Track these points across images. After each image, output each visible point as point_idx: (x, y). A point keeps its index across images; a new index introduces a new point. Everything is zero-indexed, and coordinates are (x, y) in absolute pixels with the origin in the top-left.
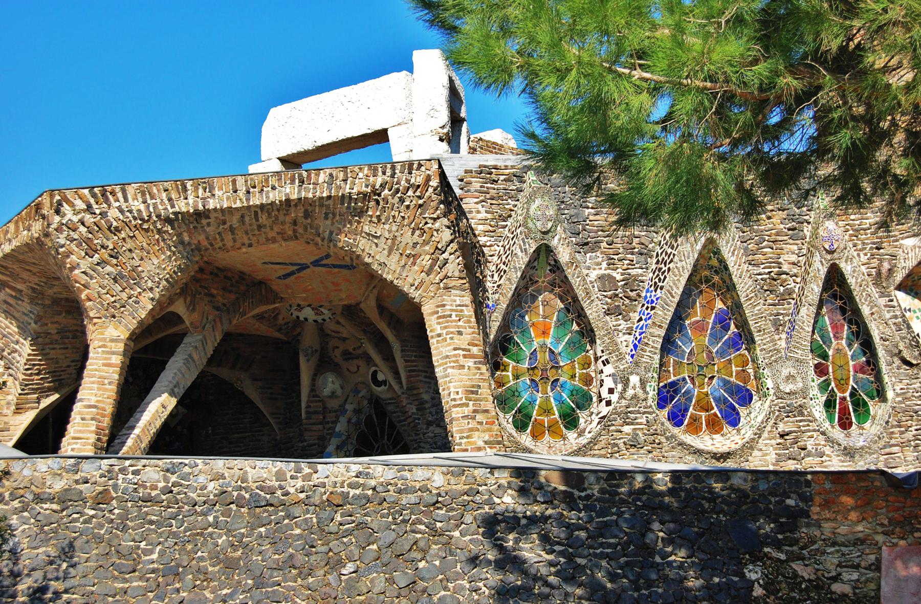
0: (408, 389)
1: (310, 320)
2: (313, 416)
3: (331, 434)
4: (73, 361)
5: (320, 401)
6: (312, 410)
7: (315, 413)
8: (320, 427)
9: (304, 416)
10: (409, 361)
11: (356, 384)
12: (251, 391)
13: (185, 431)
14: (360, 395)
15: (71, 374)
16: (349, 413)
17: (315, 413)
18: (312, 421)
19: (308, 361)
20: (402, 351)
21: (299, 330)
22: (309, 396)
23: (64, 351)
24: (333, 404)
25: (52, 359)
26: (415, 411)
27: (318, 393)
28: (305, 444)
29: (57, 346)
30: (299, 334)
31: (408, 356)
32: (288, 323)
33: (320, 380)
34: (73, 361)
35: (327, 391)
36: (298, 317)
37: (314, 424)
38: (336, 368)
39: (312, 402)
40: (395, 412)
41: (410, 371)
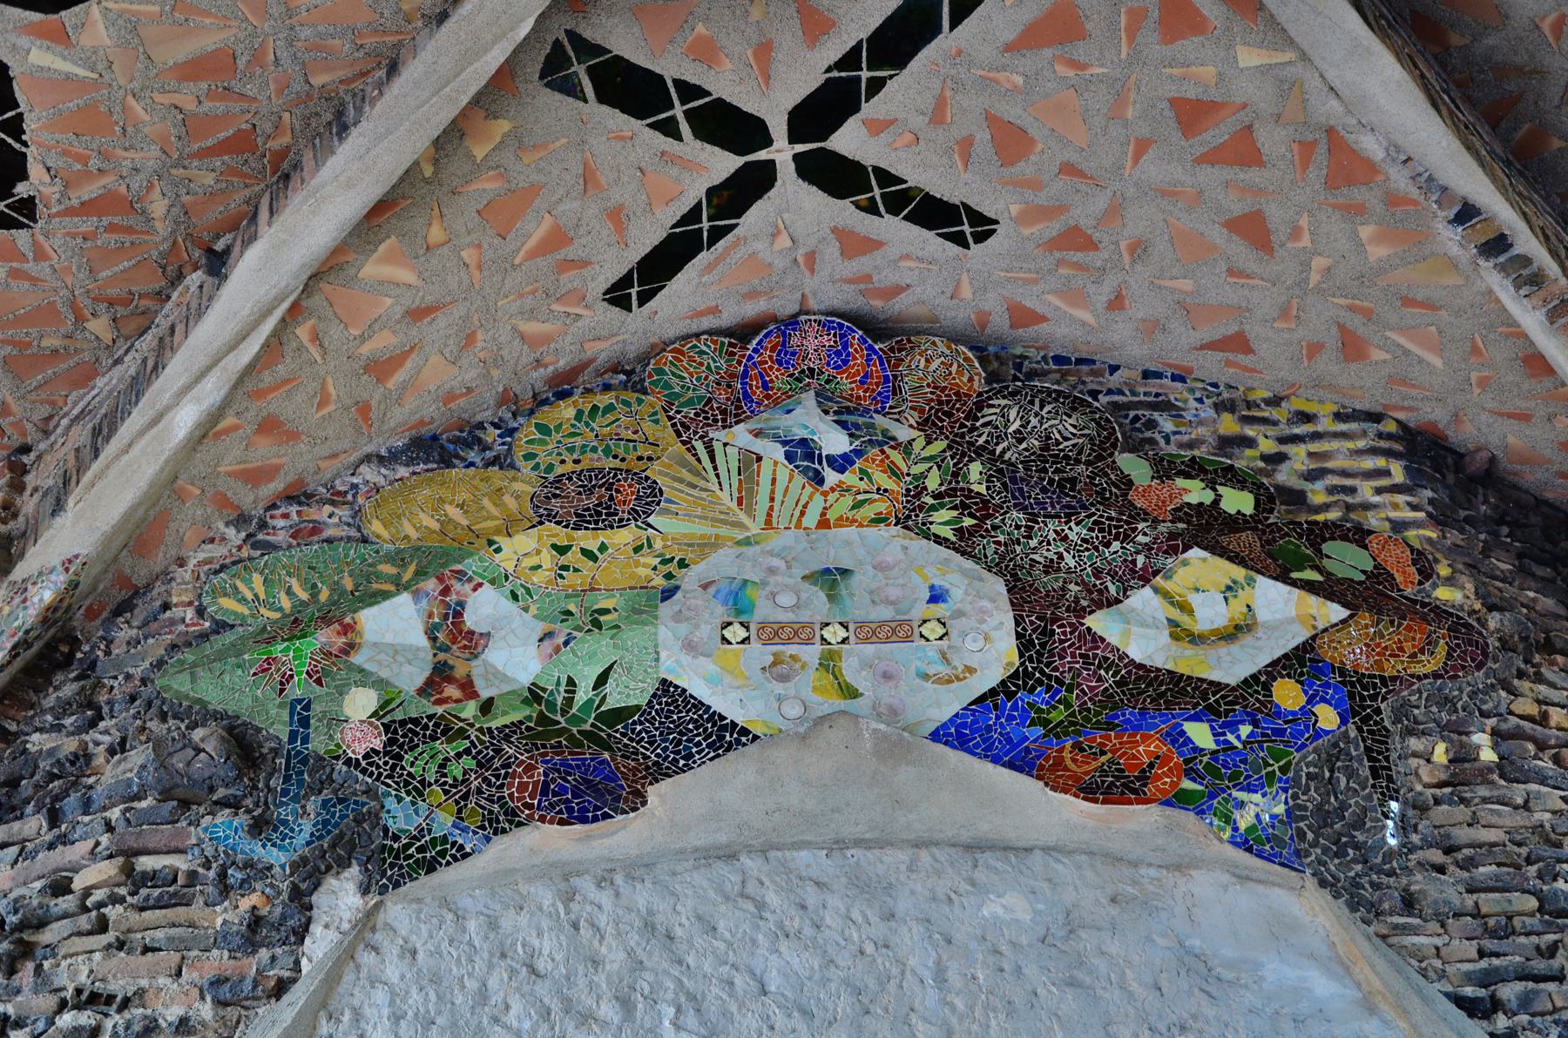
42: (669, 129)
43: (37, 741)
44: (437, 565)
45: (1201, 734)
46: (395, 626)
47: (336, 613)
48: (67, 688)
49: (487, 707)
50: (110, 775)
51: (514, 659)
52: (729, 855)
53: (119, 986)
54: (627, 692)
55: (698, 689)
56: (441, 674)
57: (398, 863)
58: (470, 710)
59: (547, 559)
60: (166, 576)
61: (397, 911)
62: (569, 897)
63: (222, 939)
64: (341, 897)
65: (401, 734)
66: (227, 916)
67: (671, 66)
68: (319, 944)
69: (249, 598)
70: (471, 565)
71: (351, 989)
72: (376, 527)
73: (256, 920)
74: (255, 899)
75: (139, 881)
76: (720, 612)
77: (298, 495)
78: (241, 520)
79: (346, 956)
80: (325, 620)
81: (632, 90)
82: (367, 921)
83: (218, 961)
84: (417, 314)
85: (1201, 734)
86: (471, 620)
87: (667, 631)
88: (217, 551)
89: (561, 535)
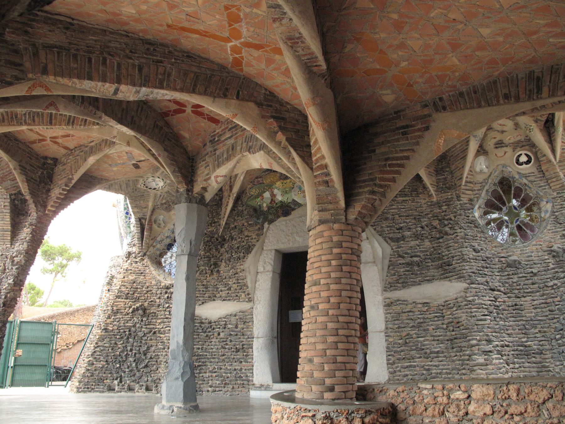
0: (560, 161)
2: (469, 184)
6: (468, 180)
9: (463, 183)
11: (498, 166)
18: (467, 188)
35: (478, 169)
37: (469, 190)
40: (535, 181)
43: (239, 208)
44: (270, 187)
46: (267, 195)
47: (260, 195)
48: (240, 203)
49: (276, 204)
50: (245, 213)
51: (279, 198)
52: (301, 217)
53: (249, 235)
54: (290, 200)
55: (296, 200)
56: (272, 200)
57: (271, 222)
58: (275, 205)
59: (281, 185)
60: (246, 189)
61: (271, 226)
62: (286, 223)
63: (257, 230)
64: (266, 225)
65: (269, 208)
66: (257, 228)
68: (265, 230)
69: (254, 192)
70: (274, 187)
71: (268, 234)
72: (264, 182)
73: (259, 228)
74: (258, 226)
75: (250, 225)
76: (298, 190)
77: (257, 178)
78: (251, 182)
79: (267, 231)
80: (261, 195)
82: (269, 227)
83: (257, 232)
86: (275, 193)
87: (293, 193)
88: (250, 186)
89: (282, 181)
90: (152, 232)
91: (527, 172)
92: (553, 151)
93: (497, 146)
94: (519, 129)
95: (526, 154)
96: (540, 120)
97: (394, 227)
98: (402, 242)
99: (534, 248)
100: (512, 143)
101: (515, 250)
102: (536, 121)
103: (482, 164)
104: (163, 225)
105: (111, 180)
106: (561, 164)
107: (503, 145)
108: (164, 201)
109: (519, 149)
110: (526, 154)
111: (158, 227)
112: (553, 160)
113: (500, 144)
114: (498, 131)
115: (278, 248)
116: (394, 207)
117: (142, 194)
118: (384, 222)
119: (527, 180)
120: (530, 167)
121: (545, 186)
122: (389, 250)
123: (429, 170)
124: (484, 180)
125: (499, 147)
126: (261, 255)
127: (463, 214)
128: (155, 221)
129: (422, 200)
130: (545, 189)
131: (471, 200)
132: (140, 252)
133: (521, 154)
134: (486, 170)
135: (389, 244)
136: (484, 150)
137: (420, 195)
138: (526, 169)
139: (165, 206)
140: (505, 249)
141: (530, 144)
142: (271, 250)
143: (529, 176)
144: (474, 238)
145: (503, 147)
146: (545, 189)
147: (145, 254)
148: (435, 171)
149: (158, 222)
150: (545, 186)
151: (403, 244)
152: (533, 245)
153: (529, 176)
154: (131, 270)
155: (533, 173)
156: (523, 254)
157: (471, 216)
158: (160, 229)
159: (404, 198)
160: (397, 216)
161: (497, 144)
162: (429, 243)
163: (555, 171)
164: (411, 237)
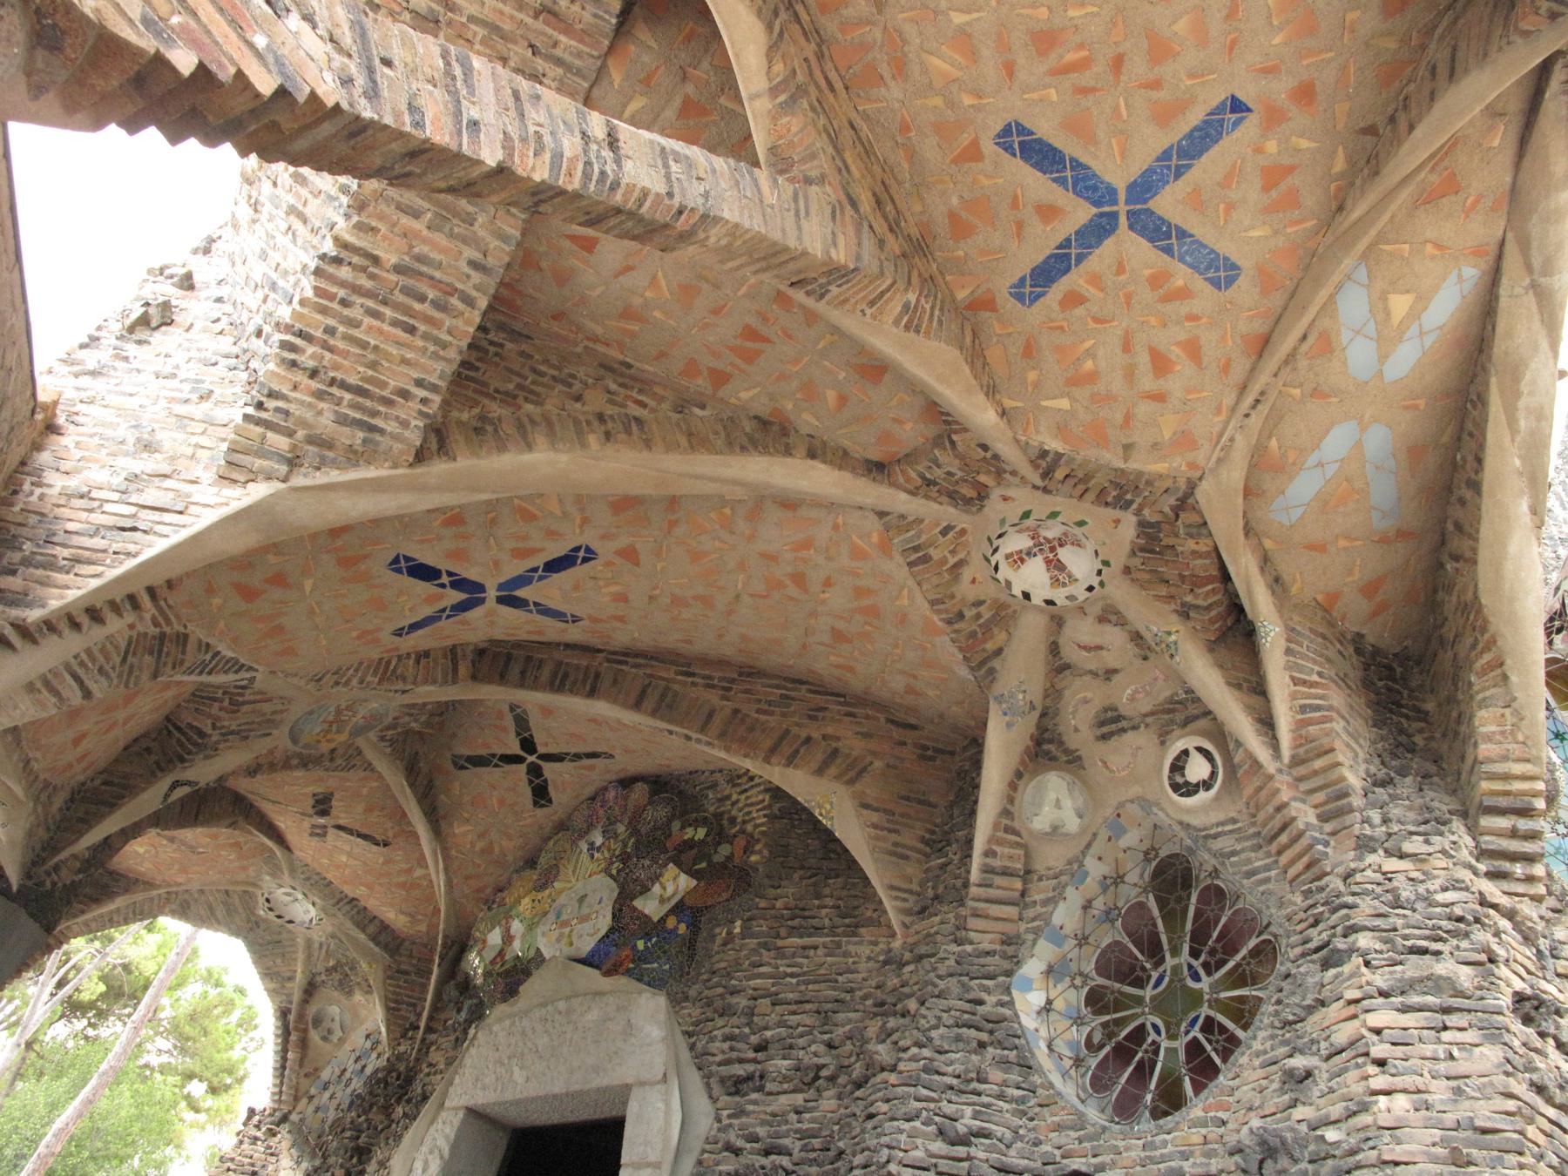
0: (1296, 761)
1: (1037, 600)
2: (999, 880)
3: (1037, 932)
4: (419, 383)
5: (1018, 845)
6: (996, 863)
7: (1006, 873)
8: (1012, 911)
9: (975, 875)
10: (1304, 683)
11: (1121, 805)
12: (851, 829)
13: (682, 928)
14: (1125, 842)
15: (405, 424)
16: (1091, 884)
17: (1006, 873)
18: (993, 893)
19: (1009, 725)
20: (1288, 652)
21: (1000, 637)
22: (996, 826)
23: (399, 333)
24: (1051, 858)
25: (364, 345)
26: (1314, 821)
27: (1016, 825)
28: (969, 948)
29: (388, 312)
30: (999, 652)
31: (1300, 669)
32: (980, 603)
33: (1028, 791)
34: (419, 383)
35: (1040, 823)
36: (1009, 584)
38: (1073, 762)
39: (1000, 842)
40: (1234, 853)
41: (1303, 709)
42: (496, 766)
45: (640, 945)
67: (483, 752)
81: (479, 761)
84: (482, 835)
85: (640, 945)
90: (311, 1053)
91: (1215, 817)
92: (1267, 723)
93: (1105, 730)
94: (1152, 656)
95: (1200, 749)
96: (1196, 607)
97: (744, 1038)
98: (754, 1096)
99: (1196, 1135)
100: (1152, 713)
101: (1121, 1144)
102: (1185, 613)
103: (1055, 804)
104: (338, 1033)
105: (159, 887)
106: (1301, 770)
107: (1124, 724)
108: (331, 963)
109: (1177, 732)
110: (1200, 749)
111: (325, 1039)
112: (1263, 755)
113: (1111, 723)
114: (1095, 674)
115: (471, 1103)
116: (762, 969)
117: (276, 937)
118: (720, 1022)
119: (1209, 850)
120: (1217, 798)
121: (1267, 868)
122: (704, 1123)
123: (894, 837)
124: (1070, 863)
125: (1112, 734)
126: (432, 1122)
127: (956, 990)
128: (317, 1022)
129: (863, 950)
130: (1267, 880)
131: (1008, 941)
132: (275, 1110)
133: (1186, 753)
134: (1072, 824)
135: (714, 1100)
136: (1067, 752)
137: (863, 931)
138: (1205, 808)
139: (336, 976)
140: (1090, 1138)
141: (1185, 710)
142: (456, 1109)
143: (1215, 836)
144: (969, 1084)
145: (1123, 730)
146: (1267, 880)
147: (284, 1119)
148: (923, 840)
149: (326, 1024)
150: (1267, 868)
151: (755, 1102)
152: (1195, 1124)
153: (1215, 836)
154: (232, 1160)
155: (1234, 821)
156: (1153, 1161)
157: (991, 1000)
158: (327, 1047)
159: (807, 941)
160: (767, 1001)
161: (1102, 724)
162: (833, 1103)
163: (1276, 802)
164: (786, 1079)
